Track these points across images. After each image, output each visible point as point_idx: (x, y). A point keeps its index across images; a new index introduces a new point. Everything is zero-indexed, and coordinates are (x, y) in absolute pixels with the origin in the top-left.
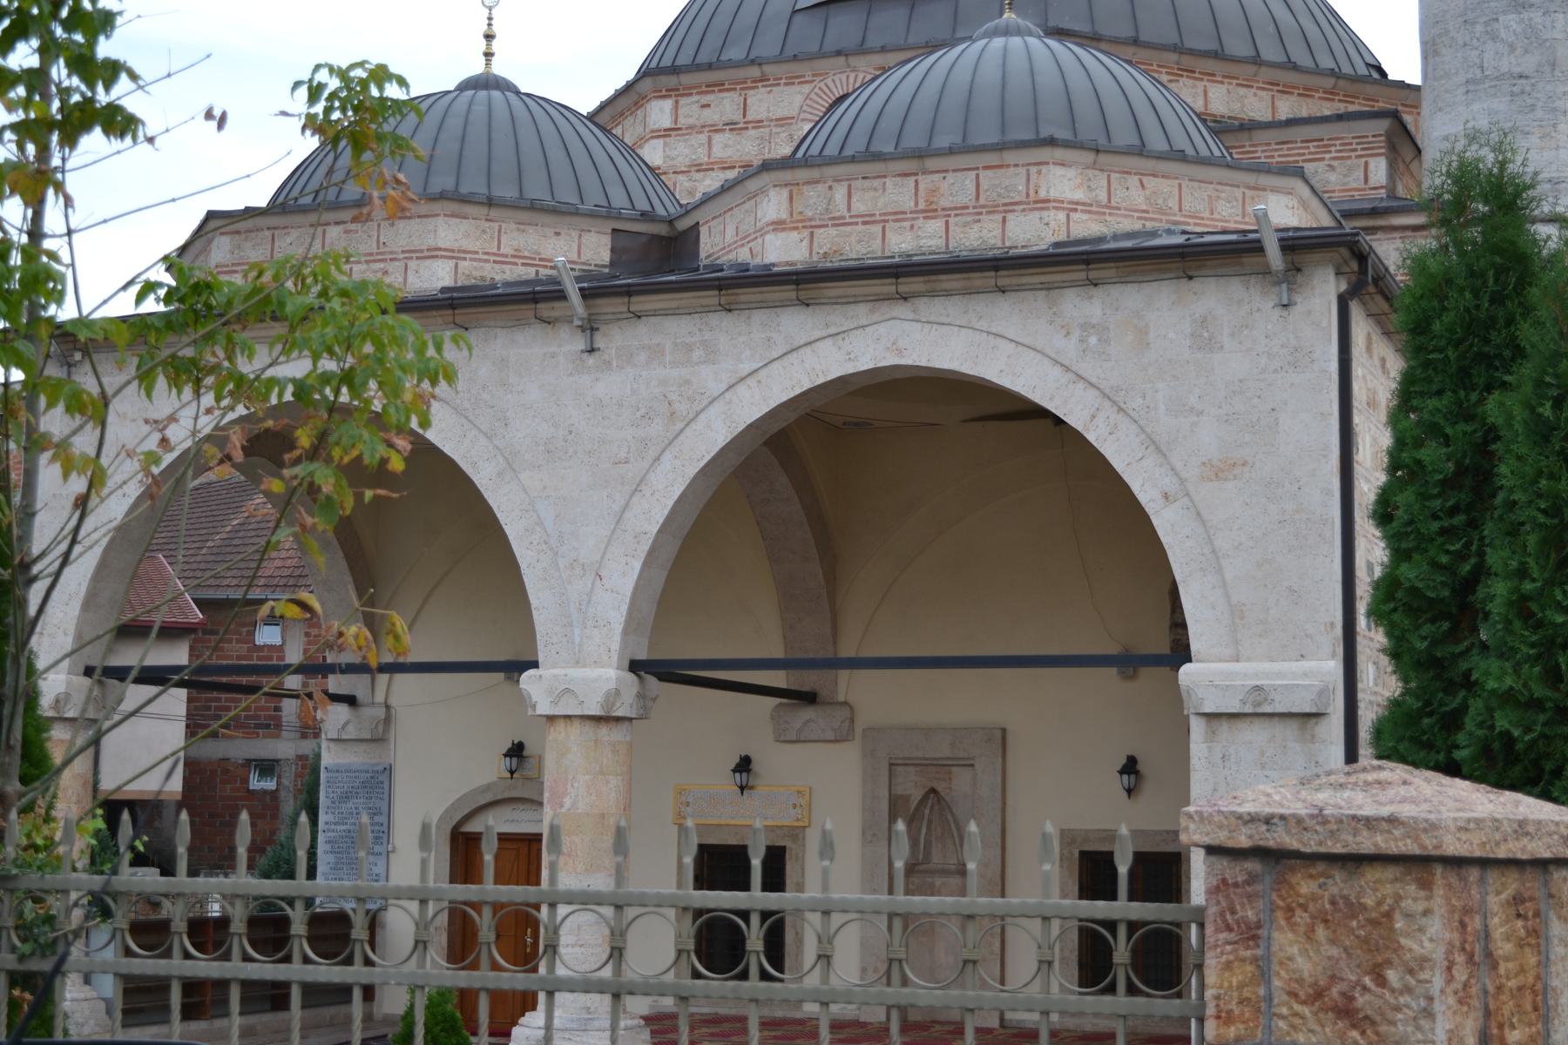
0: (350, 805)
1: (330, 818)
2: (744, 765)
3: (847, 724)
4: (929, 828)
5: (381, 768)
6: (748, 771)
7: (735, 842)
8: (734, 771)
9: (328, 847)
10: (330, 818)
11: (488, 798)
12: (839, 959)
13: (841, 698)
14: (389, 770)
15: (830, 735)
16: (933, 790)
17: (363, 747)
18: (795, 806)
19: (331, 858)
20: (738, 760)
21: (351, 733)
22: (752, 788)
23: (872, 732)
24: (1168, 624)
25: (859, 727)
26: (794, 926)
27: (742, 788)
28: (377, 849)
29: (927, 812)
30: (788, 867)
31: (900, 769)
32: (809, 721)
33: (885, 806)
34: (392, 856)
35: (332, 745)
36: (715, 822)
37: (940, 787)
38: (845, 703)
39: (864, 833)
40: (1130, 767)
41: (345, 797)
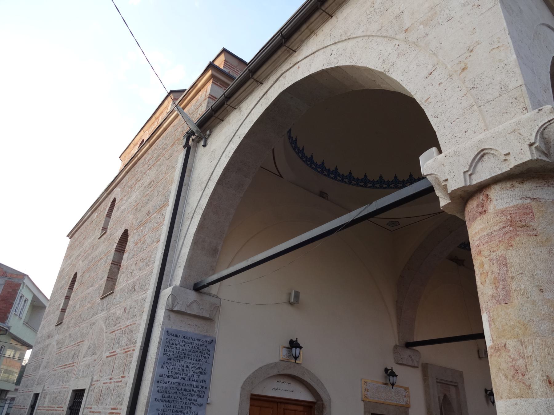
0: (183, 363)
1: (165, 371)
5: (209, 340)
9: (159, 396)
10: (165, 371)
11: (275, 372)
14: (213, 341)
15: (416, 365)
17: (196, 322)
19: (161, 405)
21: (195, 310)
28: (200, 400)
33: (437, 400)
34: (208, 407)
35: (173, 315)
41: (180, 357)
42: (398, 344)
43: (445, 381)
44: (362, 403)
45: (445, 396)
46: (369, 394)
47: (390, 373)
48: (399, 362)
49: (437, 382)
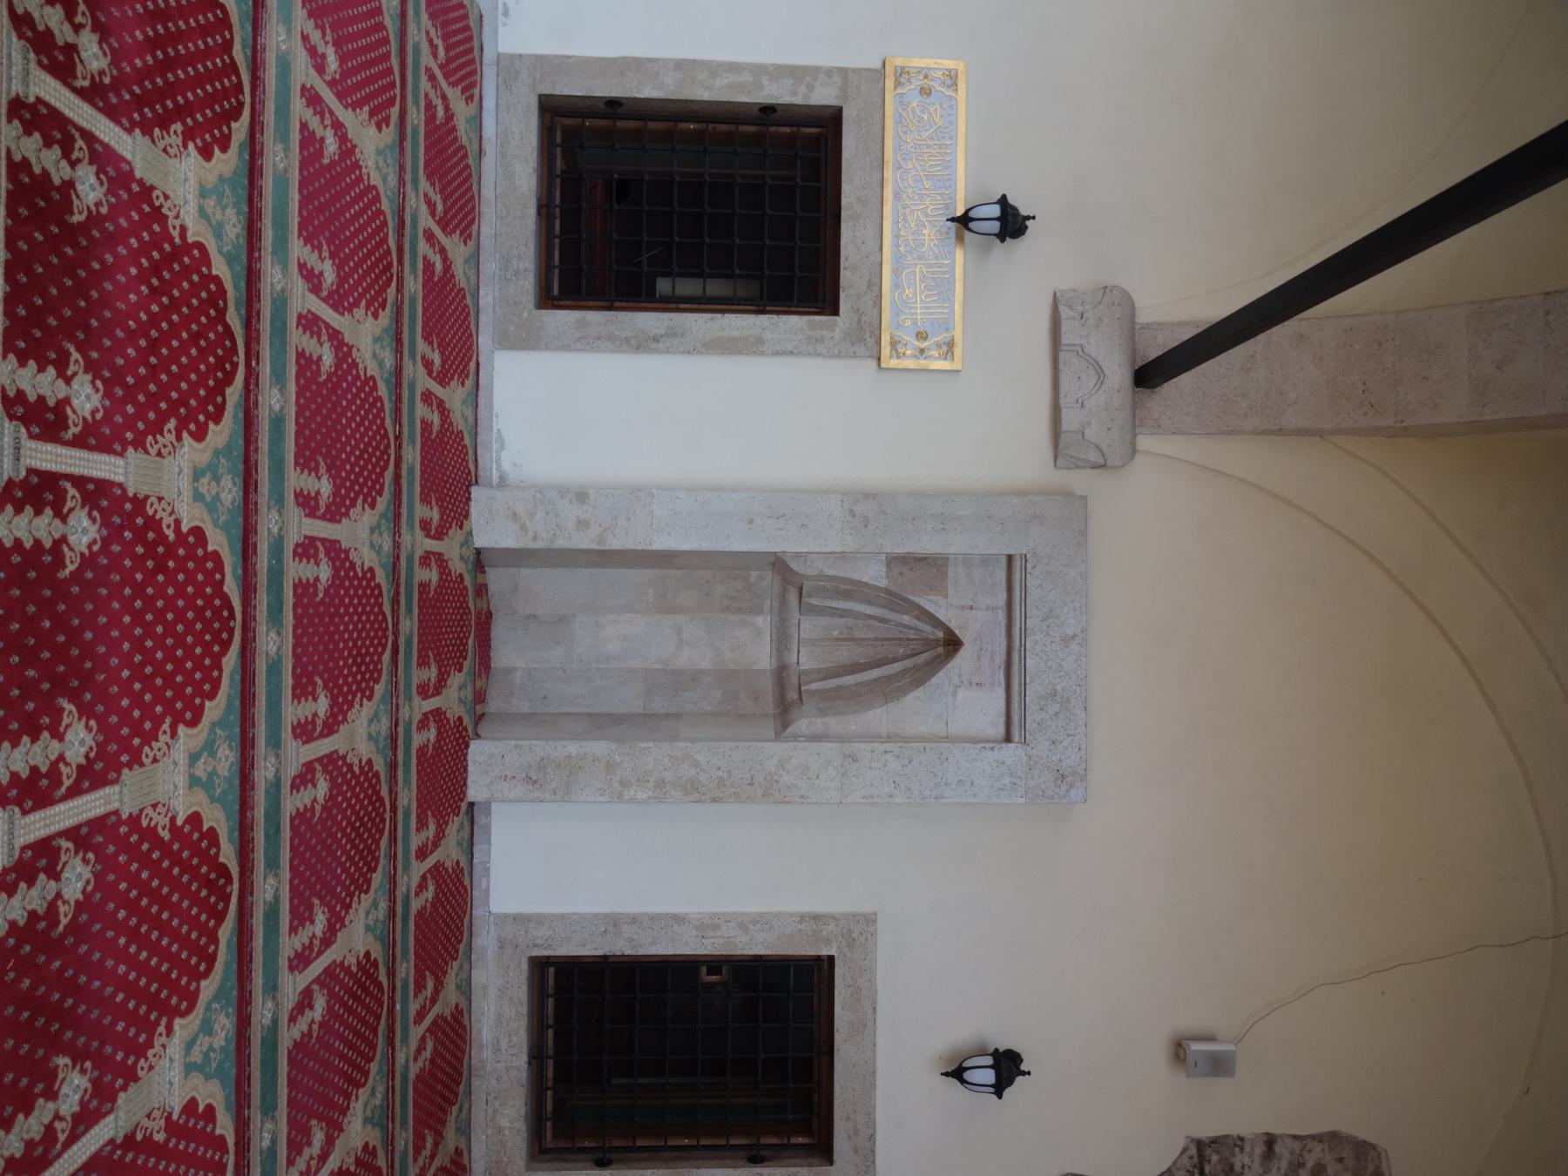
2: (1012, 224)
3: (1094, 457)
4: (869, 617)
6: (1002, 236)
7: (846, 200)
8: (1003, 201)
12: (599, 421)
13: (1144, 442)
15: (1070, 419)
16: (952, 644)
18: (921, 336)
20: (1024, 212)
22: (960, 239)
23: (1072, 513)
24: (1276, 1130)
25: (1080, 481)
26: (672, 333)
27: (964, 221)
29: (906, 619)
30: (794, 320)
31: (1001, 574)
32: (1101, 375)
33: (928, 544)
36: (889, 155)
37: (963, 659)
38: (1134, 451)
39: (869, 496)
40: (1007, 1066)
42: (1143, 317)
43: (1024, 633)
44: (877, 65)
45: (952, 644)
46: (911, 88)
47: (1012, 224)
48: (1061, 308)
49: (1010, 558)
